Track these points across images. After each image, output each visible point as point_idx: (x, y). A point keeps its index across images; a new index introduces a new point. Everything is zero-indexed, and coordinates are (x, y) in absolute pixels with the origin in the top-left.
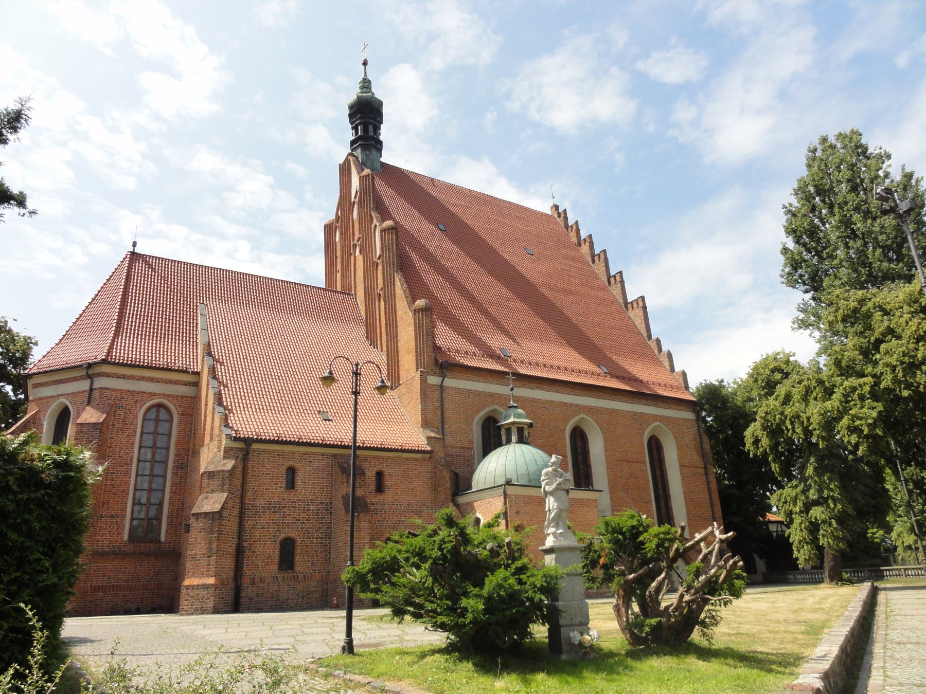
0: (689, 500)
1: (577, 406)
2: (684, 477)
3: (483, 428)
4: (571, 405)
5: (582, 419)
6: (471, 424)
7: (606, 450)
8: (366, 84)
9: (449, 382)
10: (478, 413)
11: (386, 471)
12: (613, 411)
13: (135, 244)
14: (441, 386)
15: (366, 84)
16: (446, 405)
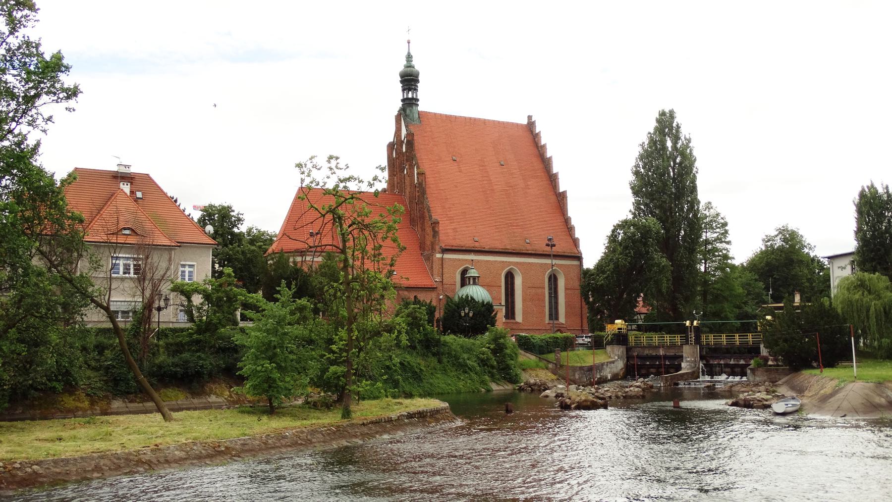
0: (568, 305)
1: (509, 262)
2: (566, 295)
3: (461, 274)
4: (506, 262)
5: (512, 268)
6: (455, 274)
7: (523, 282)
8: (409, 57)
9: (446, 256)
10: (459, 268)
11: (419, 296)
12: (529, 263)
14: (442, 258)
15: (409, 57)
16: (444, 266)
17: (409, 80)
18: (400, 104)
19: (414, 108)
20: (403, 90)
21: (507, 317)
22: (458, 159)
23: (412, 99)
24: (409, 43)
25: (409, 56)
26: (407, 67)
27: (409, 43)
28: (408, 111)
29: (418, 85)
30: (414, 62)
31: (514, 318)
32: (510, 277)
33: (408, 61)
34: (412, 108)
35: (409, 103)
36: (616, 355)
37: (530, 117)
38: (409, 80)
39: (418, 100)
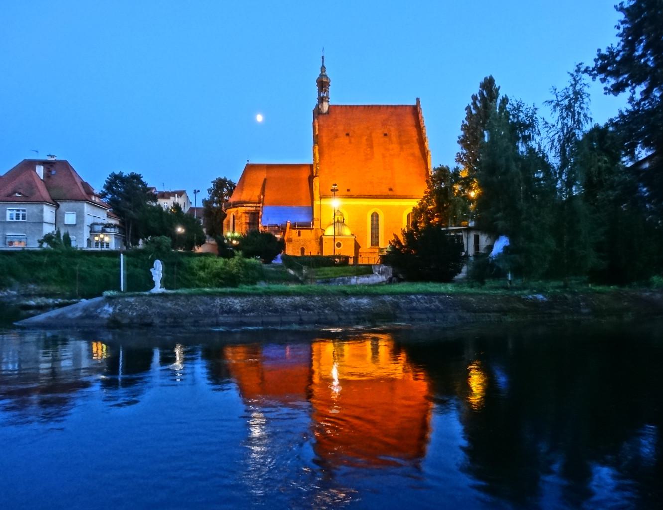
13: (248, 161)
15: (323, 68)
17: (323, 84)
18: (316, 101)
19: (324, 103)
20: (318, 92)
21: (372, 245)
22: (350, 135)
23: (323, 96)
24: (323, 59)
25: (322, 67)
26: (321, 75)
27: (323, 58)
28: (320, 106)
29: (329, 88)
30: (327, 72)
31: (378, 246)
32: (375, 217)
33: (322, 72)
34: (323, 103)
35: (321, 100)
36: (376, 271)
37: (418, 100)
38: (323, 84)
39: (329, 98)
